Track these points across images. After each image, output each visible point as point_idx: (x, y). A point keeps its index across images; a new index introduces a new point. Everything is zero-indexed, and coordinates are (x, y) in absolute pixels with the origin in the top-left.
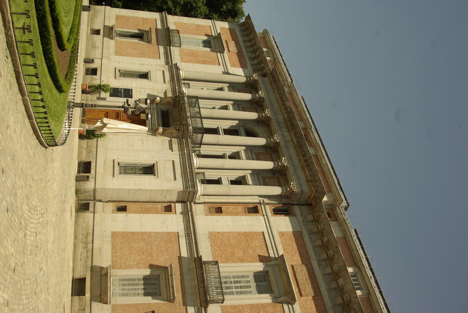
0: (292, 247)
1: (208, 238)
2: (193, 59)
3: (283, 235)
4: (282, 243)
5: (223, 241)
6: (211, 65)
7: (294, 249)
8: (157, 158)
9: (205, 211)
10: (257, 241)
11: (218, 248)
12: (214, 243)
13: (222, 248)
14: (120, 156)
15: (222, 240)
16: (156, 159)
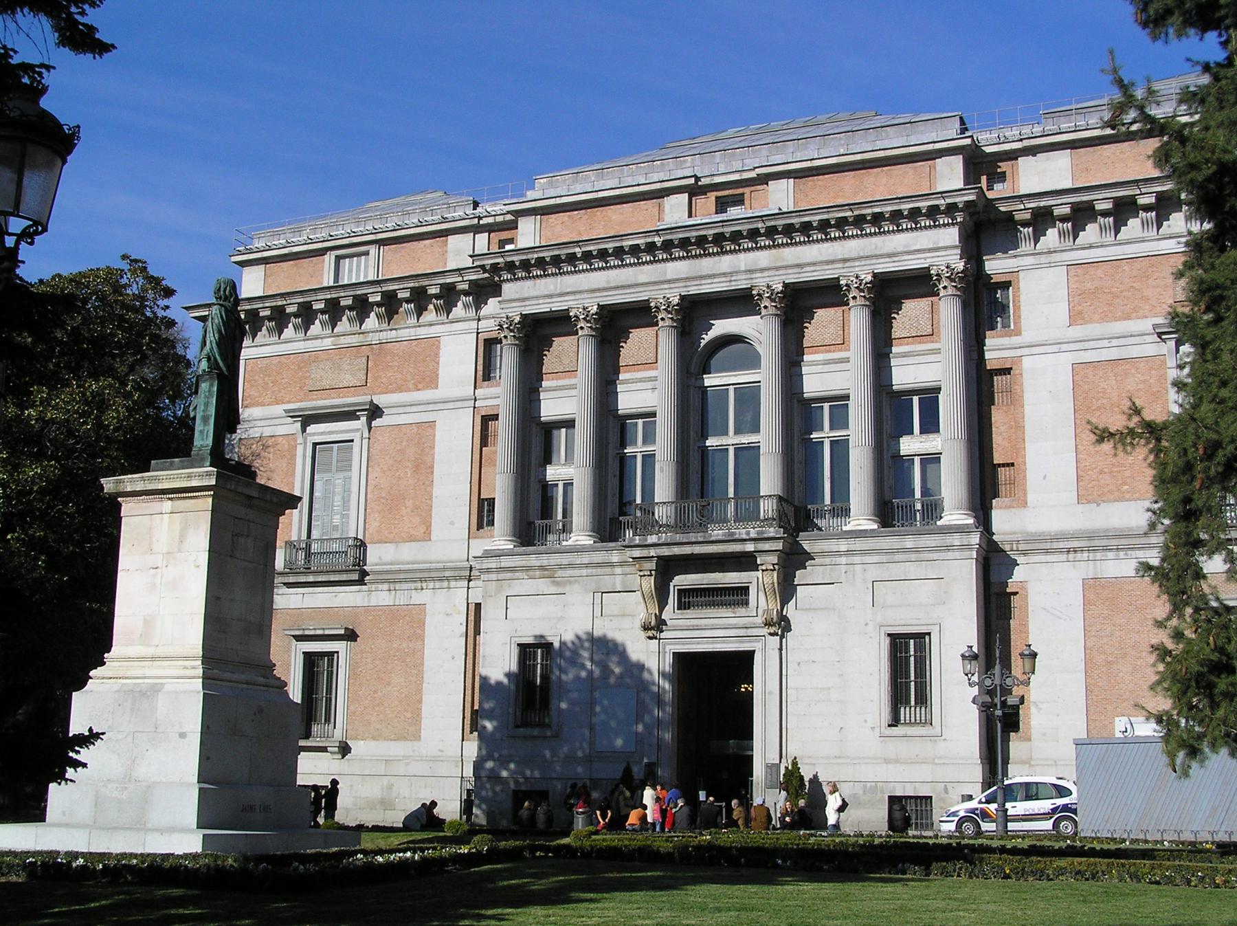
0: (1118, 297)
1: (1098, 505)
2: (409, 503)
3: (1080, 313)
4: (1105, 318)
5: (1106, 470)
6: (433, 448)
7: (1122, 292)
8: (866, 624)
9: (1010, 507)
10: (1103, 385)
11: (1126, 484)
12: (1110, 492)
13: (1128, 474)
14: (866, 721)
15: (1101, 472)
16: (870, 628)
